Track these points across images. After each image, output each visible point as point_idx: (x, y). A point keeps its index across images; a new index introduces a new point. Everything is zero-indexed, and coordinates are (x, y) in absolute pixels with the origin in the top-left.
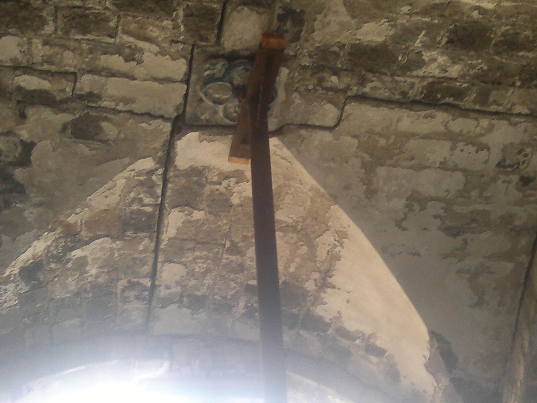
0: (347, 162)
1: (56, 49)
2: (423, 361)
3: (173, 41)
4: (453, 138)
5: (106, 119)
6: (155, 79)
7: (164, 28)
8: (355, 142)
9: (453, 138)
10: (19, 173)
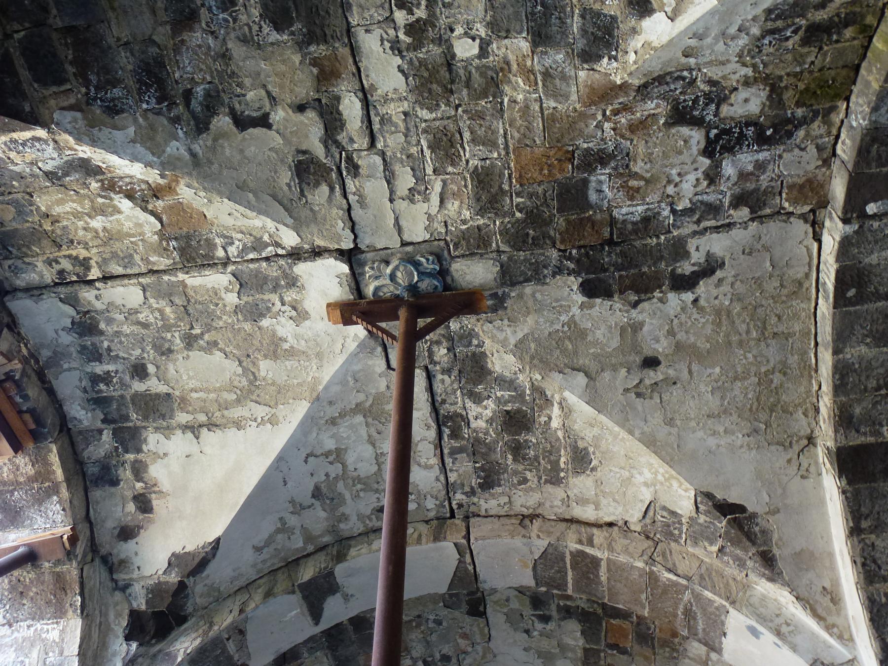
0: (358, 391)
1: (402, 126)
2: (178, 550)
3: (445, 222)
5: (332, 189)
6: (397, 219)
7: (460, 213)
10: (222, 121)
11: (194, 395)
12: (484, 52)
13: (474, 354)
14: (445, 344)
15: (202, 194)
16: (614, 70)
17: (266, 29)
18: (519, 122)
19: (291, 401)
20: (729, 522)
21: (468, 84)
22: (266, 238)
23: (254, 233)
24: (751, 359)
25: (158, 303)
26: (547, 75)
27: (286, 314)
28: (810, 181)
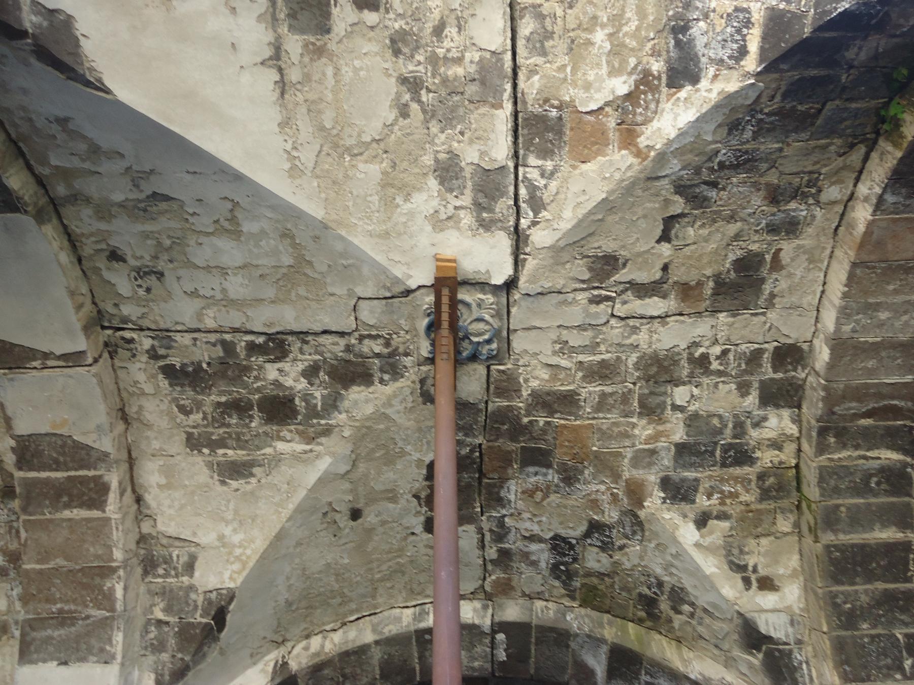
0: (329, 266)
1: (628, 342)
2: (82, 27)
4: (230, 303)
5: (583, 281)
7: (536, 378)
8: (331, 289)
9: (230, 303)
10: (679, 205)
11: (330, 71)
12: (675, 408)
13: (371, 375)
14: (386, 351)
15: (617, 176)
16: (654, 502)
17: (739, 253)
18: (616, 430)
19: (323, 195)
20: (207, 624)
21: (652, 393)
22: (544, 214)
23: (553, 205)
24: (355, 580)
25: (472, 62)
26: (653, 452)
27: (442, 208)
28: (512, 588)
